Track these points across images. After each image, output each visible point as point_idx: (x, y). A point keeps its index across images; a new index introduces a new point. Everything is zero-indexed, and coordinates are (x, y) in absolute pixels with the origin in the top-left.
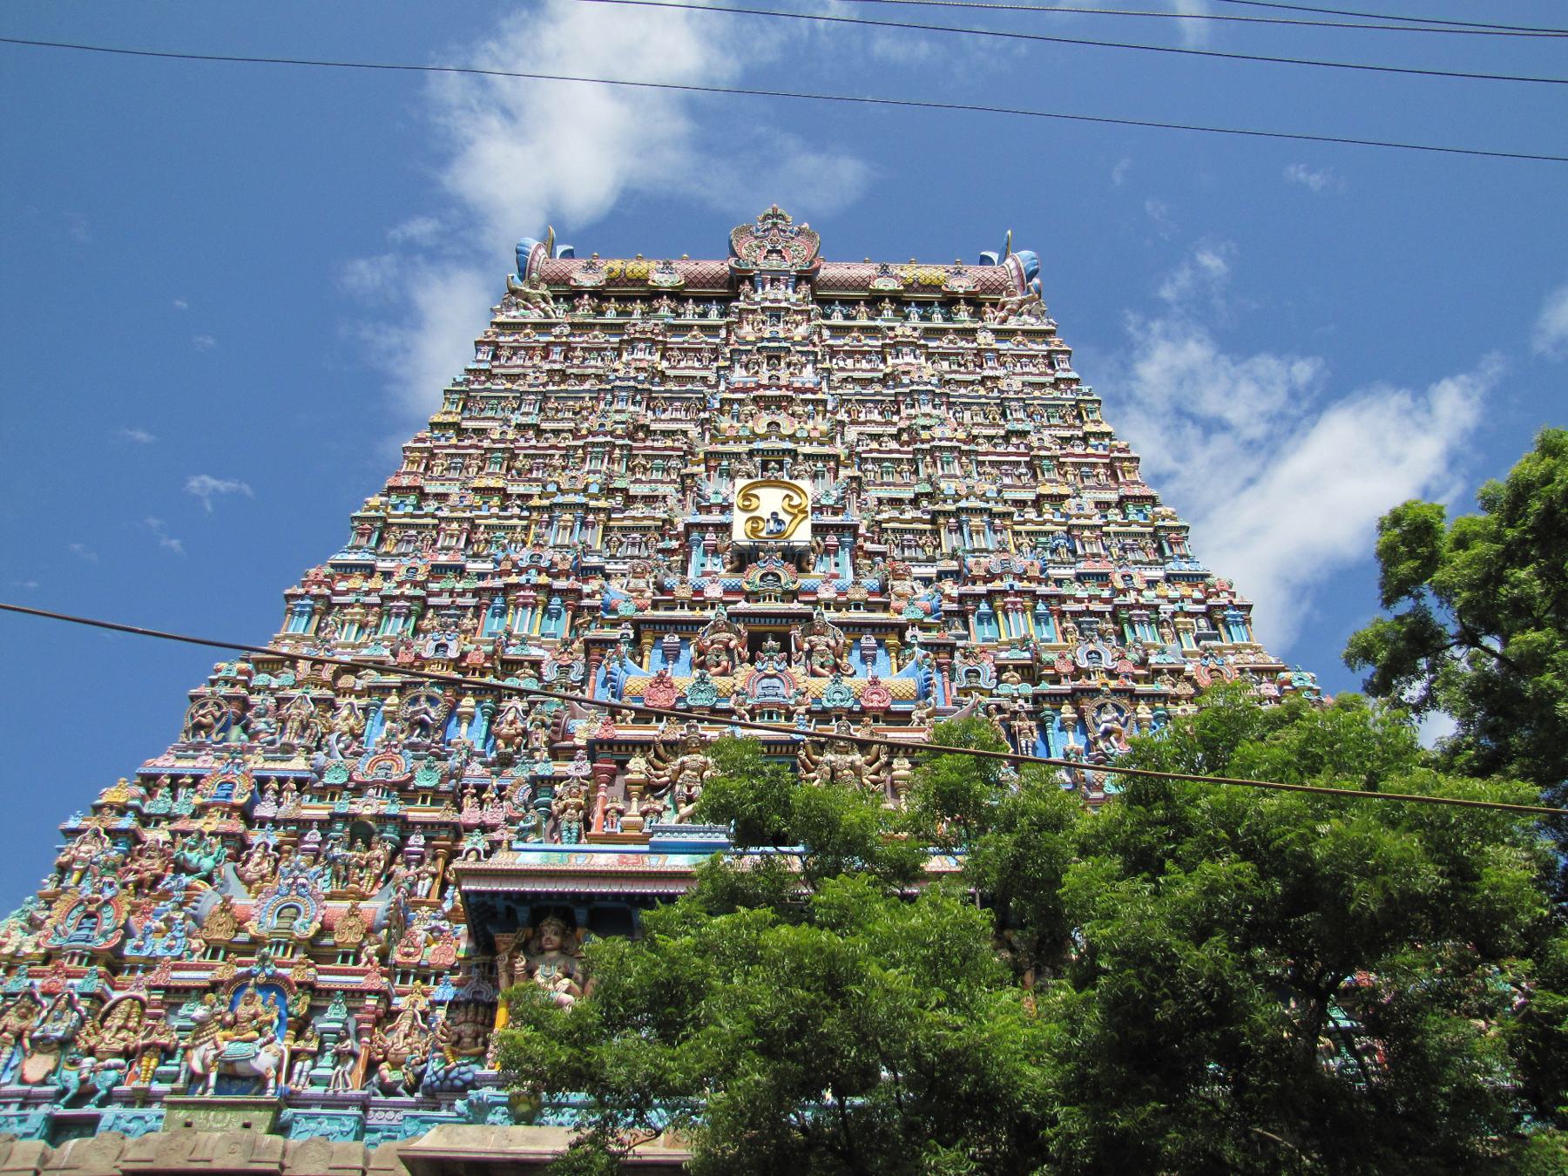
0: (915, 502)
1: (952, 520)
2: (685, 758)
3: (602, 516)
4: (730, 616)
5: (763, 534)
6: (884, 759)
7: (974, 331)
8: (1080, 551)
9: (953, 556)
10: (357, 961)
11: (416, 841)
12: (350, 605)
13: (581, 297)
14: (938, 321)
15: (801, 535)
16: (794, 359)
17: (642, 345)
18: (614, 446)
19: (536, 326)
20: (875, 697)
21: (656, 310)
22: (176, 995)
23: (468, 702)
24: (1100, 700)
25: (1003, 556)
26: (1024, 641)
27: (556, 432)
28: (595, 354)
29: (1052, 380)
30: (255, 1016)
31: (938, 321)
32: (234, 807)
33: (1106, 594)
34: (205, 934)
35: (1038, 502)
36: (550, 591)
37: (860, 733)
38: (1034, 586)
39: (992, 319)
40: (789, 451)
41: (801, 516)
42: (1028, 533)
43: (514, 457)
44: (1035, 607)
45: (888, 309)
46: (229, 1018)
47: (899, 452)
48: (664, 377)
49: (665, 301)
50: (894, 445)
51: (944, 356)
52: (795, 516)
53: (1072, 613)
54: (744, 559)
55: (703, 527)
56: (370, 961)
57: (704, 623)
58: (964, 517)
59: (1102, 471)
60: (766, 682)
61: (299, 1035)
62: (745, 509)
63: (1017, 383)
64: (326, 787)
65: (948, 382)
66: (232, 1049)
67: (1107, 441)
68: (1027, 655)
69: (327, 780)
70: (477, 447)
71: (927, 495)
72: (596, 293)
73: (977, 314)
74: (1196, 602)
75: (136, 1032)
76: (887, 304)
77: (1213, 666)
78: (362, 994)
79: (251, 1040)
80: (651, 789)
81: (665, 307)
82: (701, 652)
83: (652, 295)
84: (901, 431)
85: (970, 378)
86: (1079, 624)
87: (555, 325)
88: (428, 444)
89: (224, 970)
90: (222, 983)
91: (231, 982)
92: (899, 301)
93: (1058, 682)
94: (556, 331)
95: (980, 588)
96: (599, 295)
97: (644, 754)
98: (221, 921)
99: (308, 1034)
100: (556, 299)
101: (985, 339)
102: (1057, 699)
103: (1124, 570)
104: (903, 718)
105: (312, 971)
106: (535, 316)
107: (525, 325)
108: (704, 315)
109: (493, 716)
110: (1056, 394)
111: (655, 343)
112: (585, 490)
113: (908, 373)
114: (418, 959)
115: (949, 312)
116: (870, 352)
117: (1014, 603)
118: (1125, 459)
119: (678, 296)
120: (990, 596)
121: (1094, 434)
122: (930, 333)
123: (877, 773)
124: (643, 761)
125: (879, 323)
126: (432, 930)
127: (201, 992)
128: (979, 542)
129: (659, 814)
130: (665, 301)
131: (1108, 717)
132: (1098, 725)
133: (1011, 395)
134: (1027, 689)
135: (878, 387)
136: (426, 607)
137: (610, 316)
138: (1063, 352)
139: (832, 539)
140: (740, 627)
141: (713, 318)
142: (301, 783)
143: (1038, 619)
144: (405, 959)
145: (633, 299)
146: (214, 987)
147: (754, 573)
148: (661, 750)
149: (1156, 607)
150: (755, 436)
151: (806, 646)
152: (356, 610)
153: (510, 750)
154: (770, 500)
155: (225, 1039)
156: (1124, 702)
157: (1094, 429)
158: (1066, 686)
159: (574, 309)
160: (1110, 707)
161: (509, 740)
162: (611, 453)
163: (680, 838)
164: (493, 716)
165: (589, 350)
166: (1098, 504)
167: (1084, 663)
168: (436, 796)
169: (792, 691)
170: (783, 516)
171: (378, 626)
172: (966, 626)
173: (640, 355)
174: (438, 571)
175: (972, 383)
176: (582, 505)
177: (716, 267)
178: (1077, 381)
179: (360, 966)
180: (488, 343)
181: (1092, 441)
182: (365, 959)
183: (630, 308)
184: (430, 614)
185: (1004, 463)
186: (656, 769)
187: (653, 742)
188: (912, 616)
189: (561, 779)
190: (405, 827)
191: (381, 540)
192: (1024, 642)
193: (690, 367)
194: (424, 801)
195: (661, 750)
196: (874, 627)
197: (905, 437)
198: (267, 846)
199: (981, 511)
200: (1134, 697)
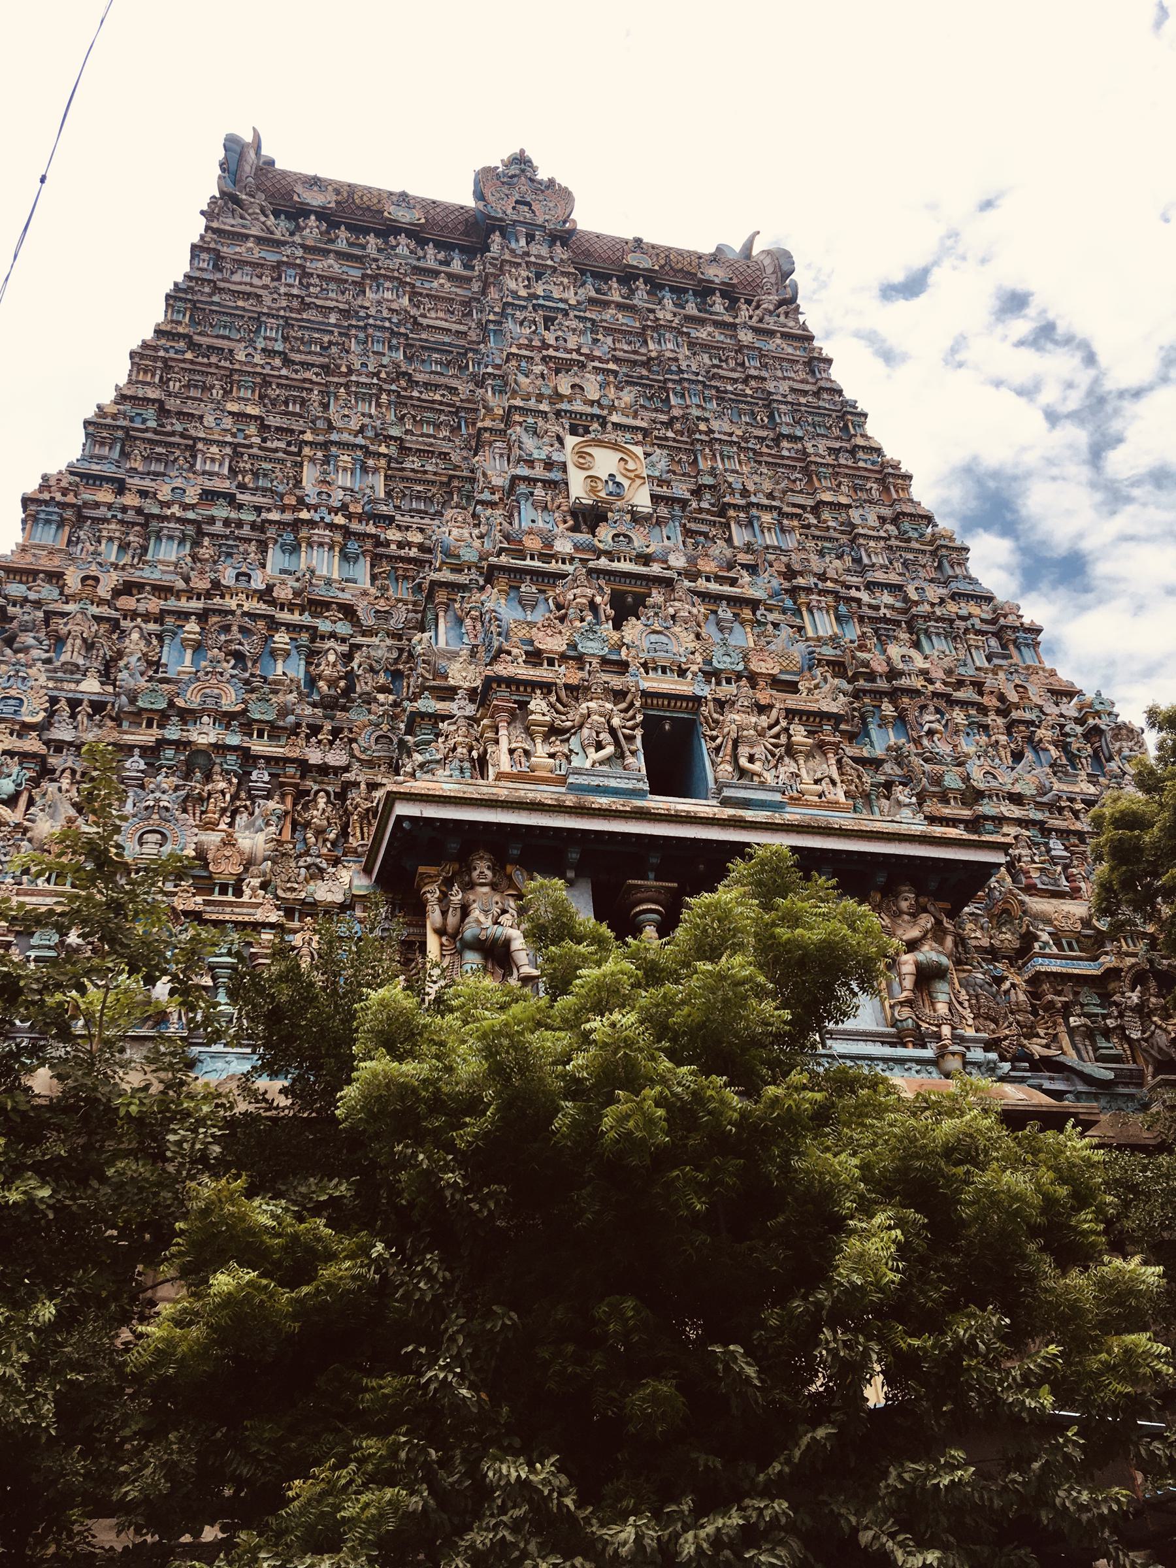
1: (742, 515)
2: (591, 704)
3: (383, 462)
4: (590, 572)
5: (603, 494)
6: (784, 723)
8: (866, 560)
10: (238, 892)
11: (260, 777)
12: (105, 520)
13: (307, 217)
14: (691, 309)
15: (641, 499)
18: (381, 389)
19: (259, 240)
21: (394, 248)
23: (281, 638)
24: (922, 701)
26: (834, 638)
29: (815, 388)
31: (691, 309)
32: (26, 727)
33: (898, 605)
35: (816, 509)
36: (347, 532)
38: (838, 588)
40: (598, 417)
41: (639, 481)
42: (814, 537)
44: (836, 609)
47: (675, 440)
49: (402, 239)
52: (633, 480)
54: (588, 517)
56: (253, 895)
58: (754, 512)
59: (875, 486)
60: (654, 638)
62: (581, 467)
63: (784, 387)
64: (142, 710)
65: (714, 376)
69: (140, 704)
70: (218, 367)
71: (710, 487)
72: (322, 215)
73: (732, 307)
74: (982, 620)
77: (1018, 682)
80: (554, 732)
81: (403, 246)
82: (559, 607)
85: (735, 375)
86: (876, 631)
87: (284, 243)
88: (161, 353)
93: (873, 680)
100: (276, 214)
101: (746, 337)
102: (878, 694)
103: (916, 583)
105: (199, 899)
107: (247, 237)
108: (447, 263)
109: (312, 656)
111: (403, 284)
114: (303, 895)
122: (689, 319)
123: (777, 736)
124: (544, 704)
126: (308, 868)
128: (771, 539)
129: (568, 758)
130: (402, 239)
131: (932, 718)
132: (922, 726)
136: (200, 533)
137: (341, 245)
140: (602, 582)
141: (456, 266)
142: (98, 707)
143: (838, 619)
144: (288, 895)
145: (366, 231)
147: (605, 533)
149: (952, 621)
150: (557, 396)
152: (113, 526)
153: (332, 692)
154: (605, 462)
156: (942, 704)
159: (299, 229)
160: (932, 709)
161: (332, 683)
163: (595, 781)
164: (312, 656)
168: (274, 731)
170: (619, 479)
171: (145, 549)
173: (388, 295)
174: (208, 496)
176: (361, 447)
179: (245, 899)
180: (208, 250)
181: (861, 455)
182: (247, 892)
183: (362, 241)
184: (206, 541)
185: (779, 465)
186: (558, 712)
189: (444, 718)
190: (248, 758)
191: (125, 455)
193: (436, 318)
194: (260, 736)
195: (563, 693)
197: (678, 426)
198: (74, 772)
199: (771, 508)
200: (952, 702)
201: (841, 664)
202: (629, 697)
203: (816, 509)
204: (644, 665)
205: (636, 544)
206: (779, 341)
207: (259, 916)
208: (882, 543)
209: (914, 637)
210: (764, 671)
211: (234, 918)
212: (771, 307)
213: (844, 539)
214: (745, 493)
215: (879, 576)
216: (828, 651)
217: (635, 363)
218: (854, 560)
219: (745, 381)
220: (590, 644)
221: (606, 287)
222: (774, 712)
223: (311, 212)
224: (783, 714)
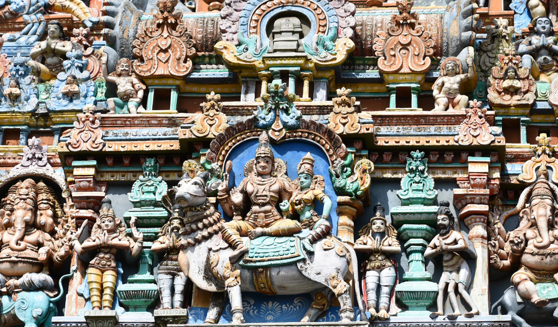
10: (427, 101)
22: (117, 167)
30: (282, 194)
34: (144, 69)
46: (237, 198)
56: (451, 102)
61: (360, 227)
66: (263, 249)
75: (53, 233)
78: (459, 154)
79: (290, 233)
89: (208, 123)
90: (204, 142)
91: (222, 139)
98: (164, 44)
99: (377, 225)
105: (367, 116)
127: (169, 163)
144: (508, 100)
146: (192, 147)
155: (243, 233)
182: (441, 100)
207: (463, 135)
211: (423, 142)
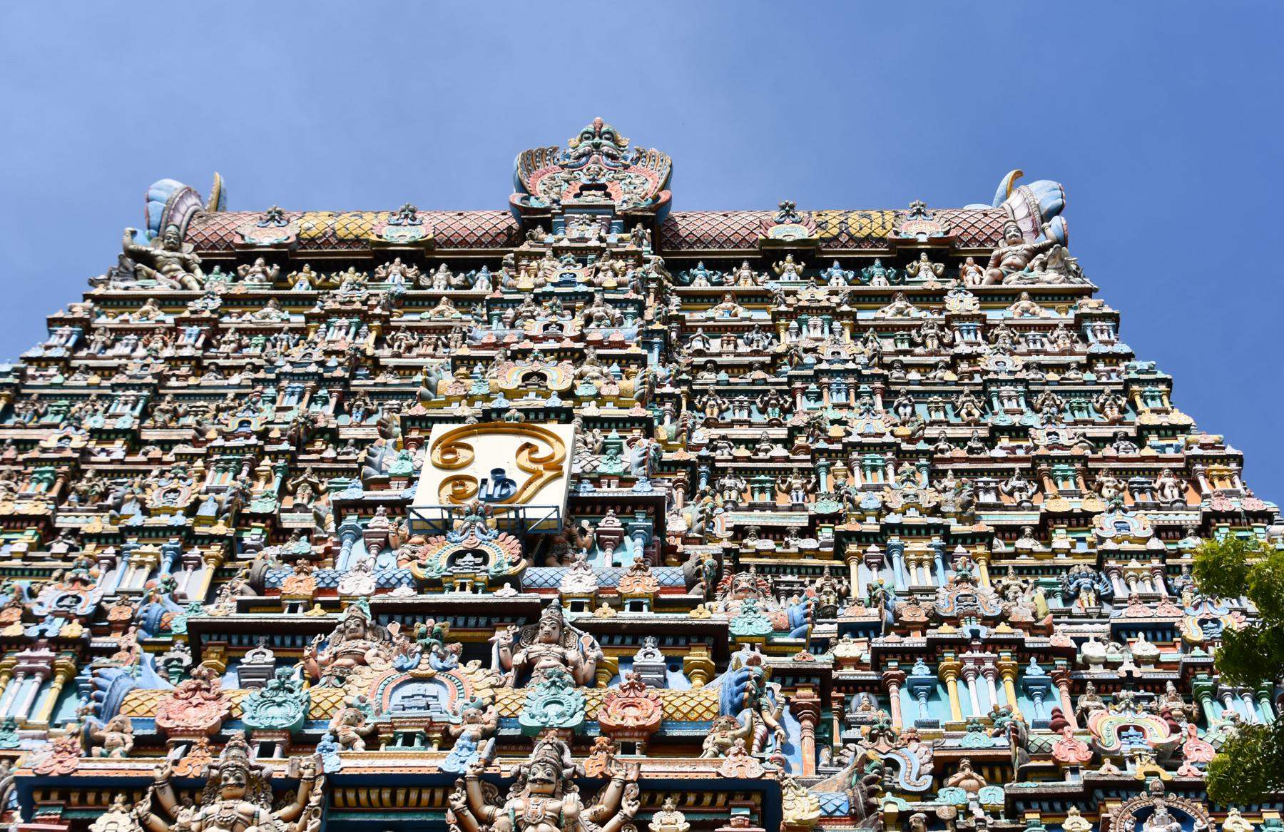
0: (808, 531)
1: (873, 548)
3: (215, 549)
6: (629, 808)
7: (944, 292)
9: (874, 601)
14: (879, 282)
16: (596, 310)
17: (344, 321)
19: (164, 302)
20: (631, 711)
24: (1141, 800)
25: (966, 589)
27: (166, 445)
28: (260, 339)
33: (1170, 655)
35: (1042, 531)
37: (590, 766)
38: (1019, 634)
39: (974, 276)
41: (548, 474)
43: (77, 474)
45: (790, 270)
48: (376, 367)
50: (779, 451)
51: (885, 330)
53: (1097, 682)
55: (365, 508)
57: (327, 628)
58: (894, 540)
59: (1170, 481)
67: (1181, 439)
68: (1002, 741)
76: (788, 263)
83: (372, 257)
84: (795, 431)
85: (932, 360)
87: (194, 298)
92: (813, 259)
94: (198, 305)
95: (916, 640)
96: (285, 259)
97: (130, 802)
100: (207, 268)
101: (961, 303)
104: (693, 746)
106: (162, 286)
107: (144, 299)
110: (1089, 376)
111: (366, 318)
112: (191, 510)
113: (814, 350)
115: (901, 274)
116: (750, 328)
117: (980, 661)
118: (1214, 459)
119: (422, 256)
120: (932, 652)
121: (1157, 429)
125: (772, 285)
128: (921, 578)
130: (396, 267)
133: (1003, 376)
134: (995, 796)
135: (759, 374)
138: (1104, 317)
139: (611, 522)
140: (394, 628)
143: (1024, 689)
148: (168, 798)
151: (519, 658)
157: (1154, 420)
158: (1073, 783)
160: (1161, 812)
162: (255, 463)
165: (251, 332)
166: (1160, 531)
167: (1112, 743)
169: (459, 704)
172: (885, 704)
175: (934, 367)
176: (177, 530)
177: (489, 218)
178: (1128, 357)
180: (71, 322)
187: (151, 780)
188: (751, 631)
192: (993, 720)
195: (168, 798)
196: (663, 634)
199: (926, 531)
201: (1005, 763)
202: (302, 789)
203: (1042, 531)
204: (372, 740)
205: (491, 565)
206: (1025, 303)
208: (1156, 562)
209: (1193, 707)
210: (631, 722)
212: (1018, 261)
213: (1083, 565)
214: (885, 509)
215: (1139, 614)
216: (981, 742)
217: (750, 367)
218: (1100, 599)
219: (952, 366)
220: (274, 710)
221: (731, 278)
222: (612, 789)
223: (258, 255)
224: (633, 790)
